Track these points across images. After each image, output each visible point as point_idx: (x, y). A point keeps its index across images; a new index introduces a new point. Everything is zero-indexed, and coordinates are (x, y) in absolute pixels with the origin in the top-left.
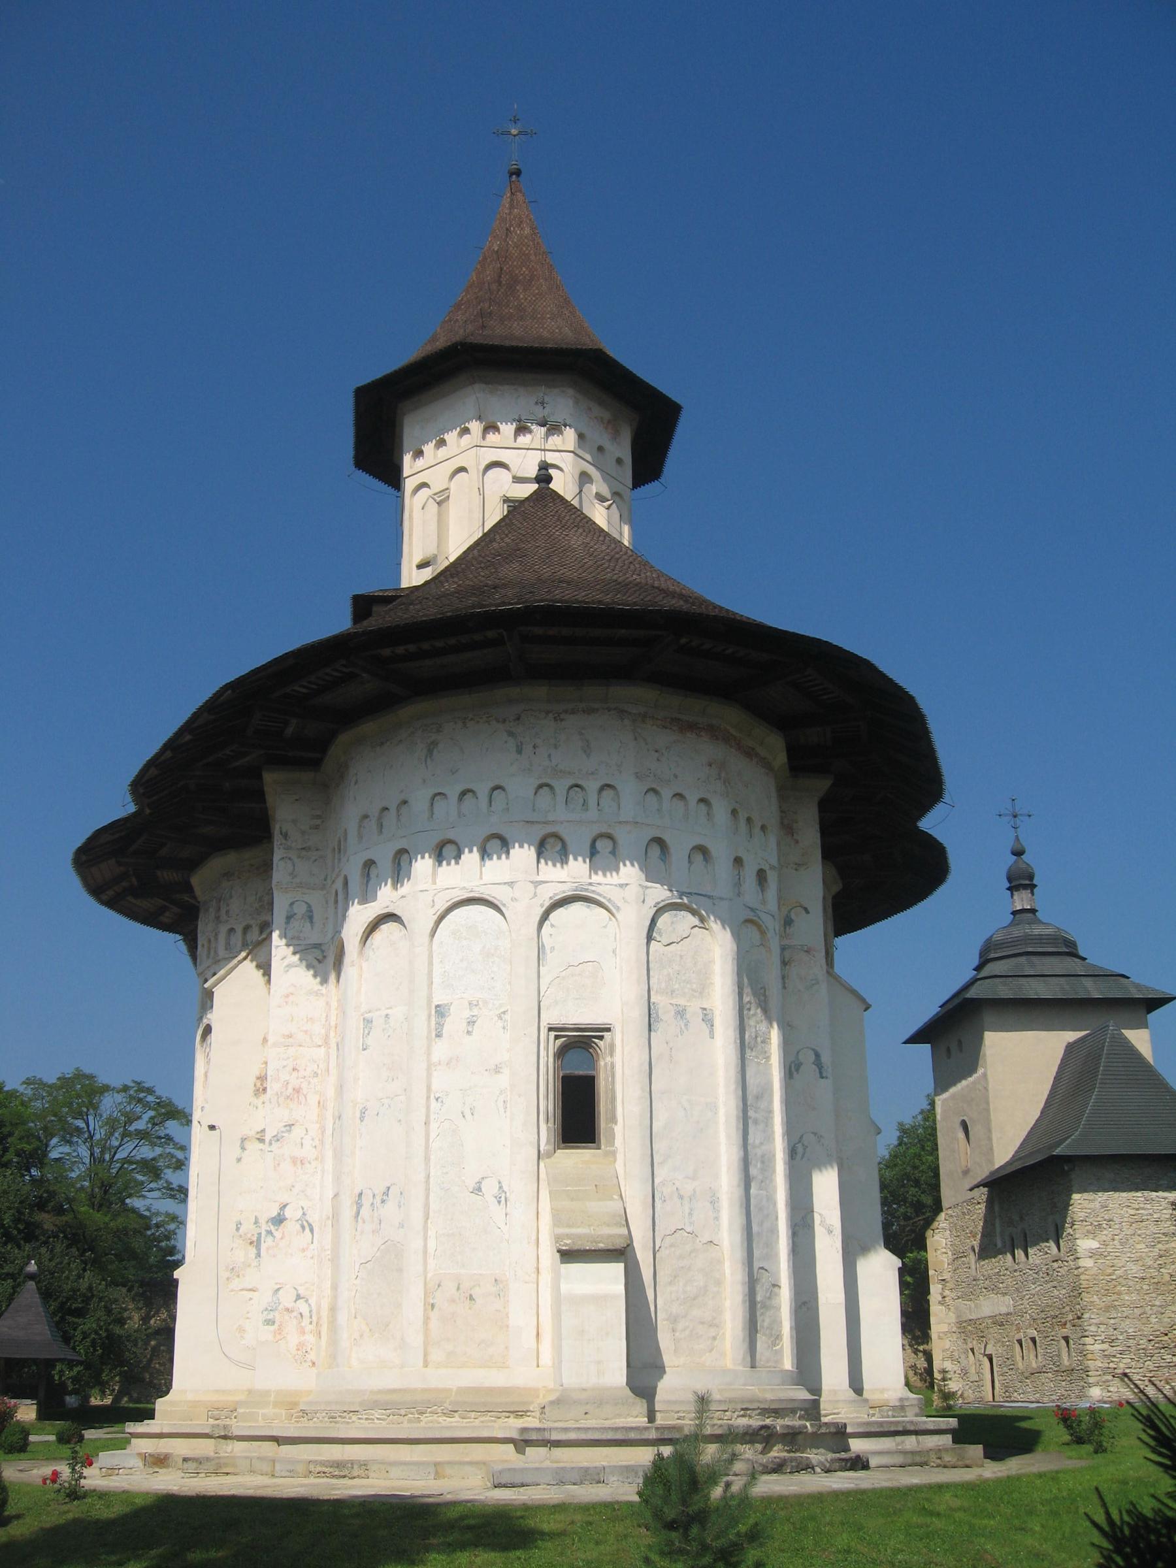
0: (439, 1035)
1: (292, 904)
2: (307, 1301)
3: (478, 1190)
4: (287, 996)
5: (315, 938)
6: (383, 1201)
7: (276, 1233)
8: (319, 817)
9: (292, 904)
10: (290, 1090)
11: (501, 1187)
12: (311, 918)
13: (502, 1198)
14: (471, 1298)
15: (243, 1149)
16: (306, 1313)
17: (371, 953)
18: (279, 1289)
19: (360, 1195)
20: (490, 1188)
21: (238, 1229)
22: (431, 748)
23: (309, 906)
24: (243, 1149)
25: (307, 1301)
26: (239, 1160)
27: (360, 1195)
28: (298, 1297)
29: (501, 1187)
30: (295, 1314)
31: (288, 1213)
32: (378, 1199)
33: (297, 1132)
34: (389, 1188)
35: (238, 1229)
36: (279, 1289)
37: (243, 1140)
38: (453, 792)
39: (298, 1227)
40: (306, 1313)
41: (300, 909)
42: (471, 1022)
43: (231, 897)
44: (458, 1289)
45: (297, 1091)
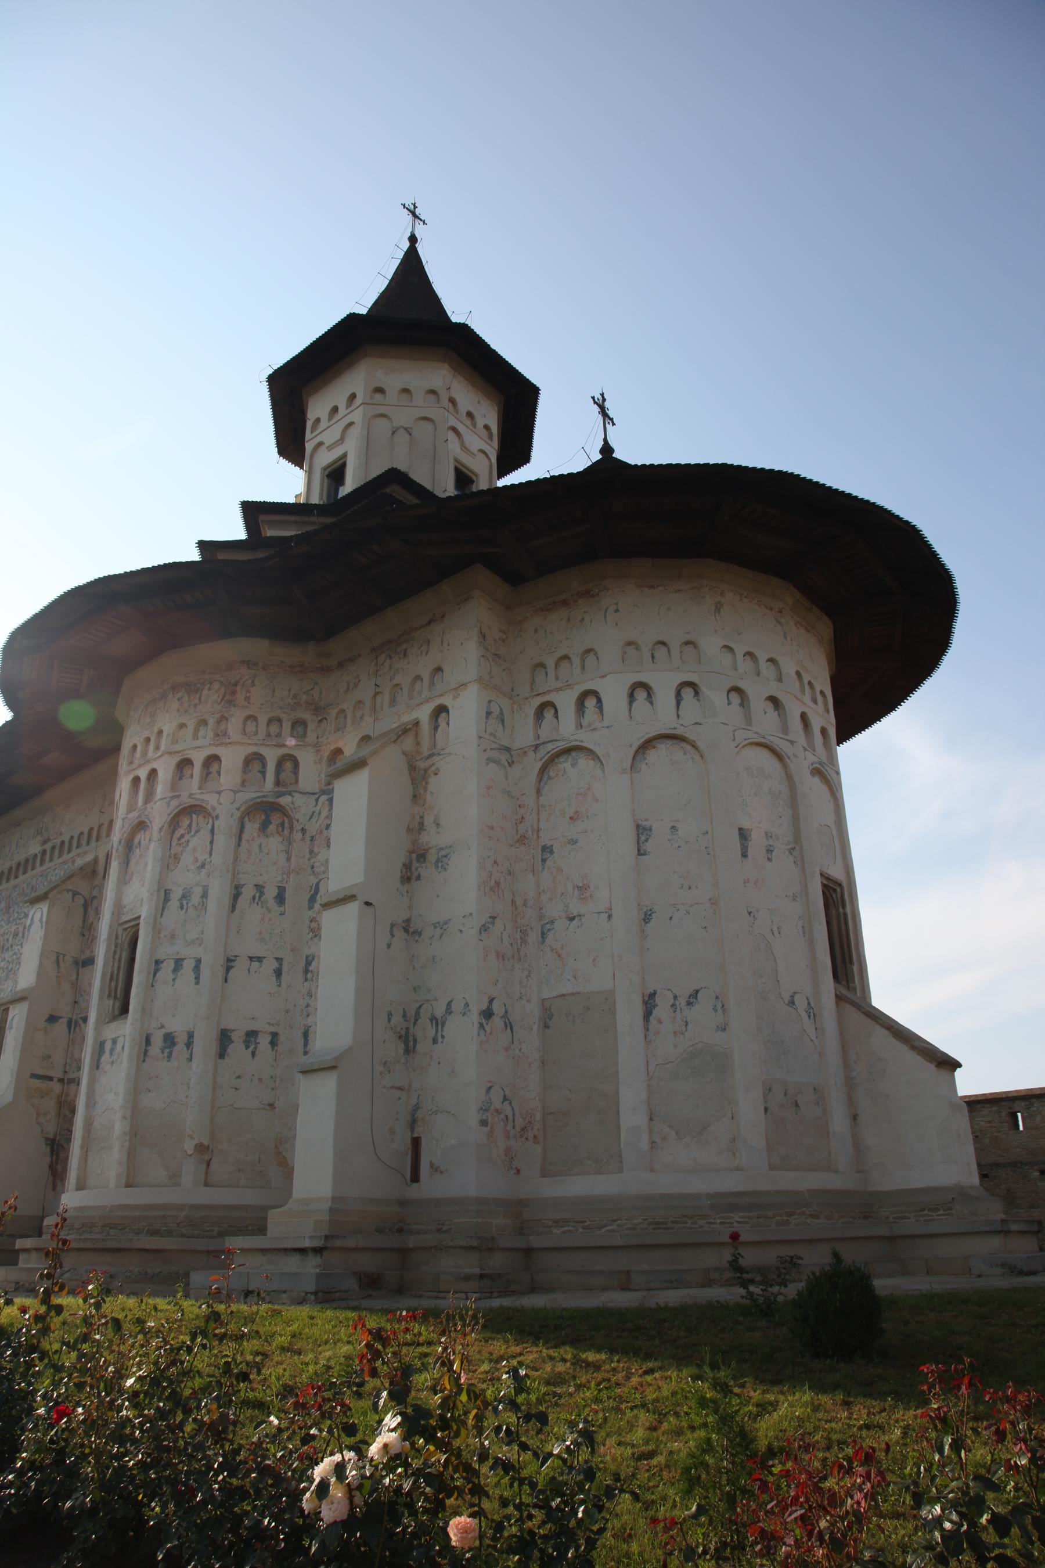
0: (744, 855)
1: (490, 702)
2: (510, 1103)
3: (792, 1003)
4: (489, 788)
5: (505, 742)
6: (689, 1004)
7: (487, 1028)
8: (504, 633)
9: (490, 702)
10: (492, 883)
11: (809, 1004)
12: (503, 721)
13: (812, 1013)
14: (797, 1104)
15: (392, 935)
16: (510, 1117)
17: (643, 767)
18: (490, 1088)
19: (653, 995)
20: (800, 1002)
21: (389, 1020)
22: (718, 607)
23: (501, 710)
24: (392, 935)
25: (510, 1103)
26: (389, 946)
27: (653, 995)
28: (505, 1099)
29: (809, 1004)
30: (502, 1116)
31: (496, 1007)
32: (682, 1001)
33: (499, 925)
34: (697, 992)
35: (389, 1020)
36: (490, 1088)
37: (392, 926)
38: (740, 650)
39: (502, 1024)
40: (510, 1117)
41: (496, 710)
42: (770, 851)
43: (253, 684)
44: (785, 1094)
45: (498, 884)
